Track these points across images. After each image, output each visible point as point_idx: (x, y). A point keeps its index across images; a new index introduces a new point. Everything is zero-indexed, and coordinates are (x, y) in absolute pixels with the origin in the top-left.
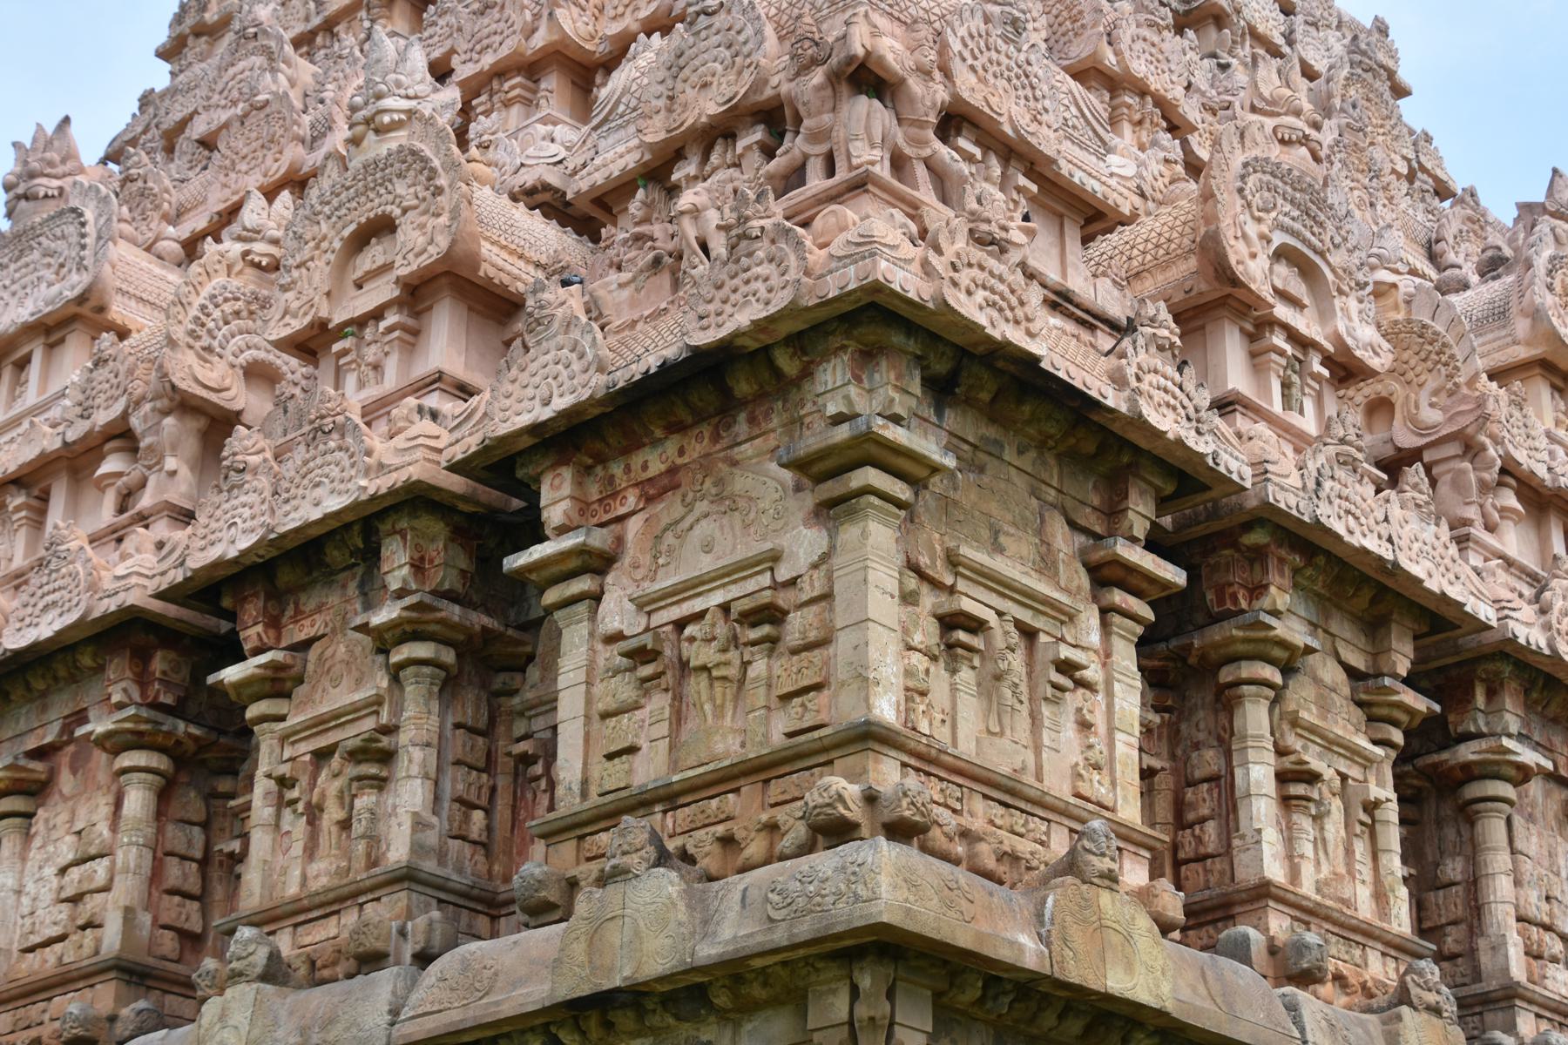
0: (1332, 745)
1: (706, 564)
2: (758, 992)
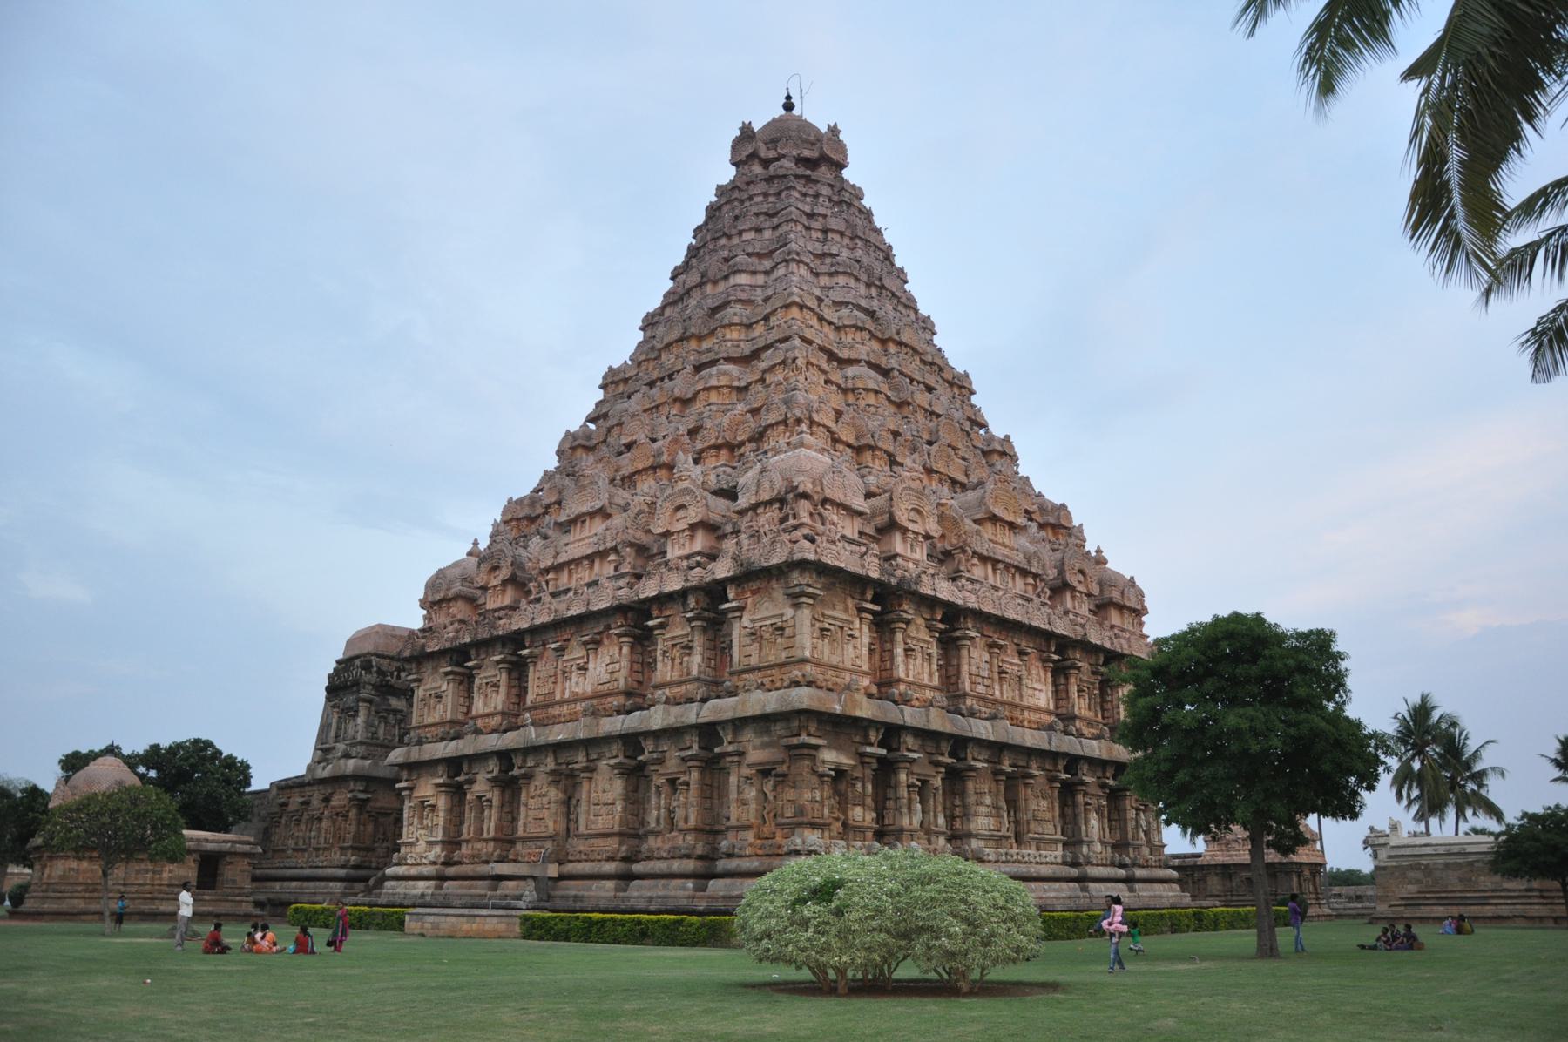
0: (919, 640)
1: (767, 614)
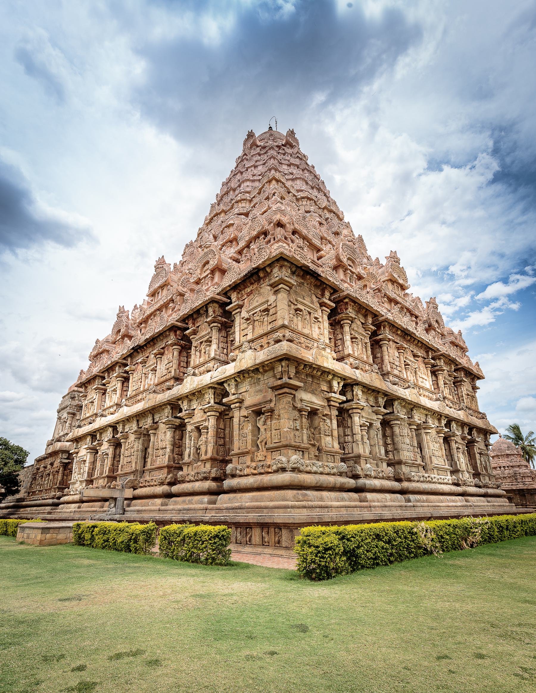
1: (257, 304)
2: (267, 368)
